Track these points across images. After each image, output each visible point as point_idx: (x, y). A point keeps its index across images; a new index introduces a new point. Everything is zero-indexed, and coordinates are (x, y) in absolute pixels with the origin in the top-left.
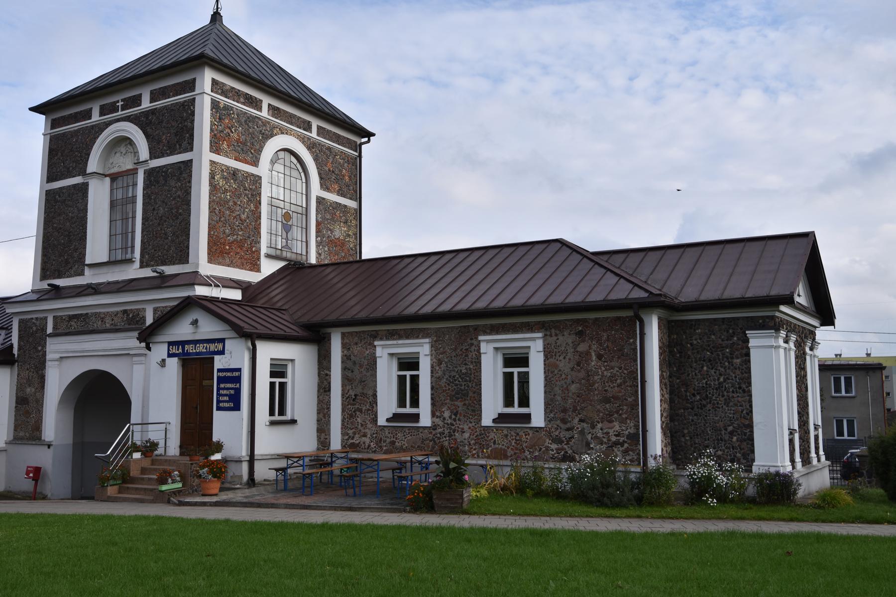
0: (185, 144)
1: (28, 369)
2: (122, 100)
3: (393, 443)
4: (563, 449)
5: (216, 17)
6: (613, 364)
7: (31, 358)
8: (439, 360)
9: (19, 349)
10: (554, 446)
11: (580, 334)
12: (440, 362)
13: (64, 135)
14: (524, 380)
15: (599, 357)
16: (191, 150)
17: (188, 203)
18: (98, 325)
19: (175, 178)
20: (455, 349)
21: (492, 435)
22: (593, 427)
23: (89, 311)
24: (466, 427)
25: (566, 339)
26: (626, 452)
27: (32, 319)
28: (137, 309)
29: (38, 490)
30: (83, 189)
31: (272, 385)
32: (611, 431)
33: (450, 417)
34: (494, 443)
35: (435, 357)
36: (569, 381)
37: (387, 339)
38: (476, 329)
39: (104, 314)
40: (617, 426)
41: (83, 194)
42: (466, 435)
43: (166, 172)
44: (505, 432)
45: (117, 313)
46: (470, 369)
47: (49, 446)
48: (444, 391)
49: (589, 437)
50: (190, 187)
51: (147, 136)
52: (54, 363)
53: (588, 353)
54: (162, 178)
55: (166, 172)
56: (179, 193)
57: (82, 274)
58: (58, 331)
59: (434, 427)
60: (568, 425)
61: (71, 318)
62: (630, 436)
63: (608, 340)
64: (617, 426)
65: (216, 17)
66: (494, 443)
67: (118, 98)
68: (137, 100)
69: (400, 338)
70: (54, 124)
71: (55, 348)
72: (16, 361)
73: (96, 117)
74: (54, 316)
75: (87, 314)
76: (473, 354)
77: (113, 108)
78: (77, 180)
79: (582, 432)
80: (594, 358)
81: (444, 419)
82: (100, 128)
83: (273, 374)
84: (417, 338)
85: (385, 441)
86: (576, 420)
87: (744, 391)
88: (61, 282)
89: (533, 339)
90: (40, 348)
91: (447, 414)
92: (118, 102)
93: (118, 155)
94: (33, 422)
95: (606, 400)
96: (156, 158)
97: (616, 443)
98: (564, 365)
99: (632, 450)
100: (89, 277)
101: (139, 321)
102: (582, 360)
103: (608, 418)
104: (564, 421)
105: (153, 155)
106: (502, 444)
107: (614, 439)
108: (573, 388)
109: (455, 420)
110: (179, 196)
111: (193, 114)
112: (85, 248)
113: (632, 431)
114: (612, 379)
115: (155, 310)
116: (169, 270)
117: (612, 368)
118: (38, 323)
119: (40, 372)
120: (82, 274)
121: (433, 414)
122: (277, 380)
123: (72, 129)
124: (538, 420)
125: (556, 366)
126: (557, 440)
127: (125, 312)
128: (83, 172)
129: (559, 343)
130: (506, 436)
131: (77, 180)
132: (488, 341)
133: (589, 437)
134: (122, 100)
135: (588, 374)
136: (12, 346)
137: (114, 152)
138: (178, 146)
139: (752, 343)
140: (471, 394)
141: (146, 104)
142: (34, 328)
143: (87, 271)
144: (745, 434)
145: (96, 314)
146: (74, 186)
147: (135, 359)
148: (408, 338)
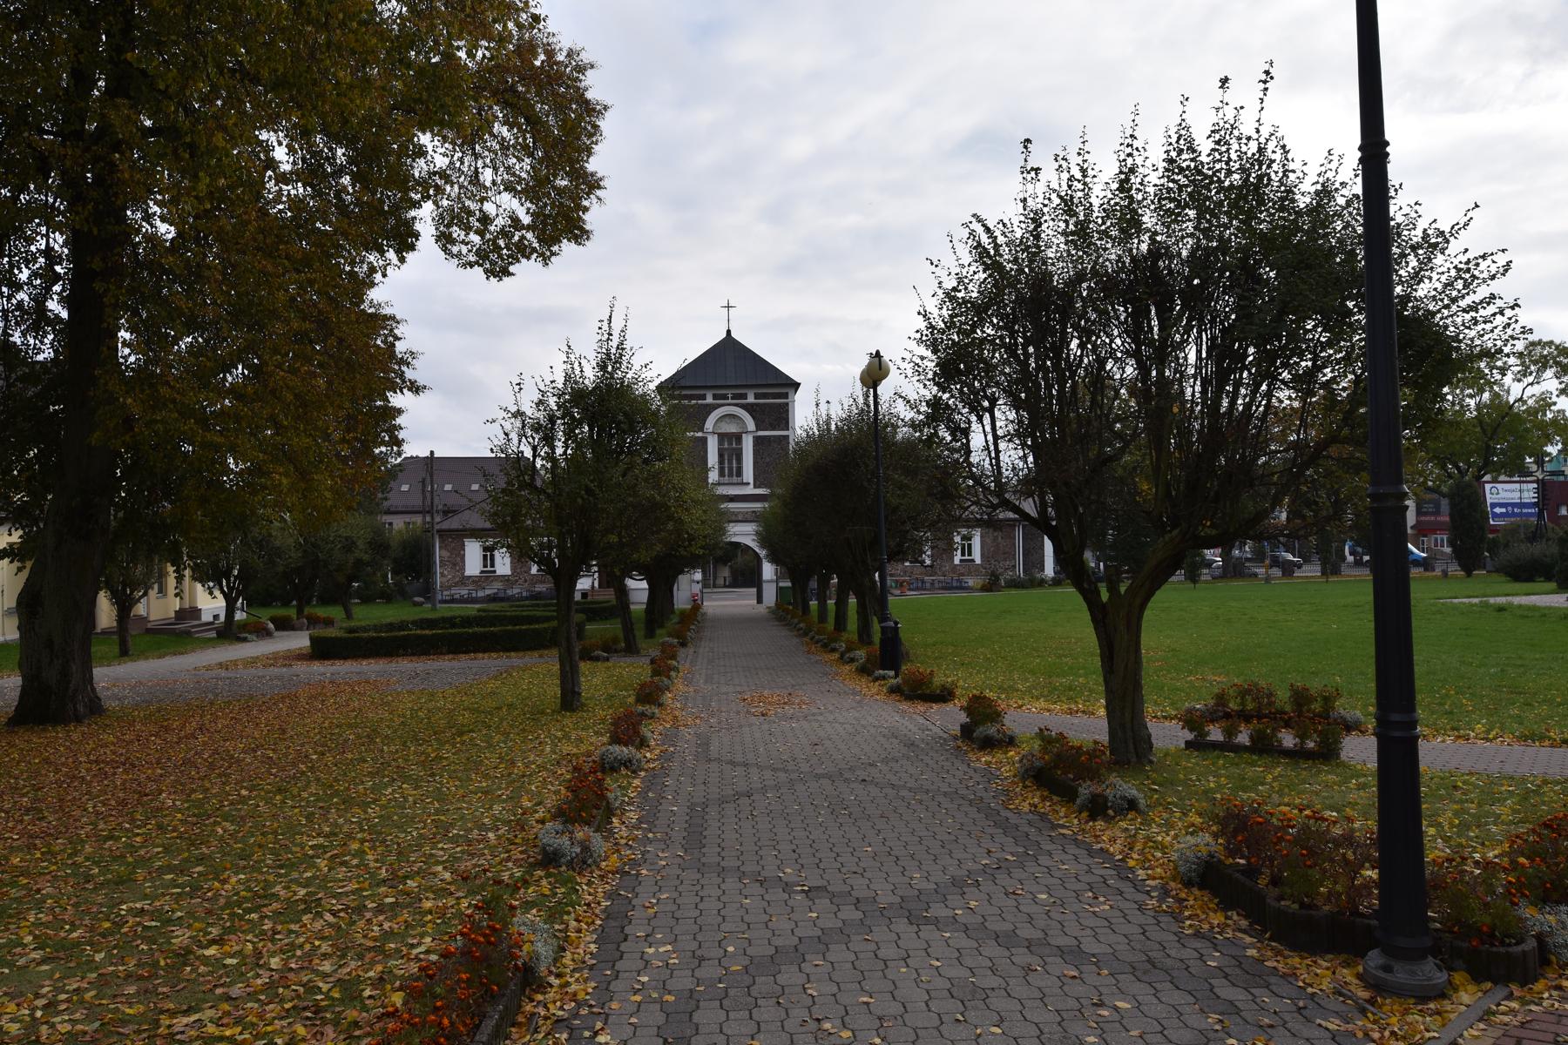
0: (782, 426)
5: (729, 332)
14: (970, 545)
18: (734, 518)
30: (704, 441)
51: (754, 418)
65: (729, 332)
67: (730, 393)
68: (744, 396)
77: (725, 397)
95: (1004, 553)
98: (988, 541)
102: (995, 539)
103: (1005, 560)
105: (758, 428)
111: (788, 411)
124: (978, 561)
128: (701, 429)
141: (751, 399)
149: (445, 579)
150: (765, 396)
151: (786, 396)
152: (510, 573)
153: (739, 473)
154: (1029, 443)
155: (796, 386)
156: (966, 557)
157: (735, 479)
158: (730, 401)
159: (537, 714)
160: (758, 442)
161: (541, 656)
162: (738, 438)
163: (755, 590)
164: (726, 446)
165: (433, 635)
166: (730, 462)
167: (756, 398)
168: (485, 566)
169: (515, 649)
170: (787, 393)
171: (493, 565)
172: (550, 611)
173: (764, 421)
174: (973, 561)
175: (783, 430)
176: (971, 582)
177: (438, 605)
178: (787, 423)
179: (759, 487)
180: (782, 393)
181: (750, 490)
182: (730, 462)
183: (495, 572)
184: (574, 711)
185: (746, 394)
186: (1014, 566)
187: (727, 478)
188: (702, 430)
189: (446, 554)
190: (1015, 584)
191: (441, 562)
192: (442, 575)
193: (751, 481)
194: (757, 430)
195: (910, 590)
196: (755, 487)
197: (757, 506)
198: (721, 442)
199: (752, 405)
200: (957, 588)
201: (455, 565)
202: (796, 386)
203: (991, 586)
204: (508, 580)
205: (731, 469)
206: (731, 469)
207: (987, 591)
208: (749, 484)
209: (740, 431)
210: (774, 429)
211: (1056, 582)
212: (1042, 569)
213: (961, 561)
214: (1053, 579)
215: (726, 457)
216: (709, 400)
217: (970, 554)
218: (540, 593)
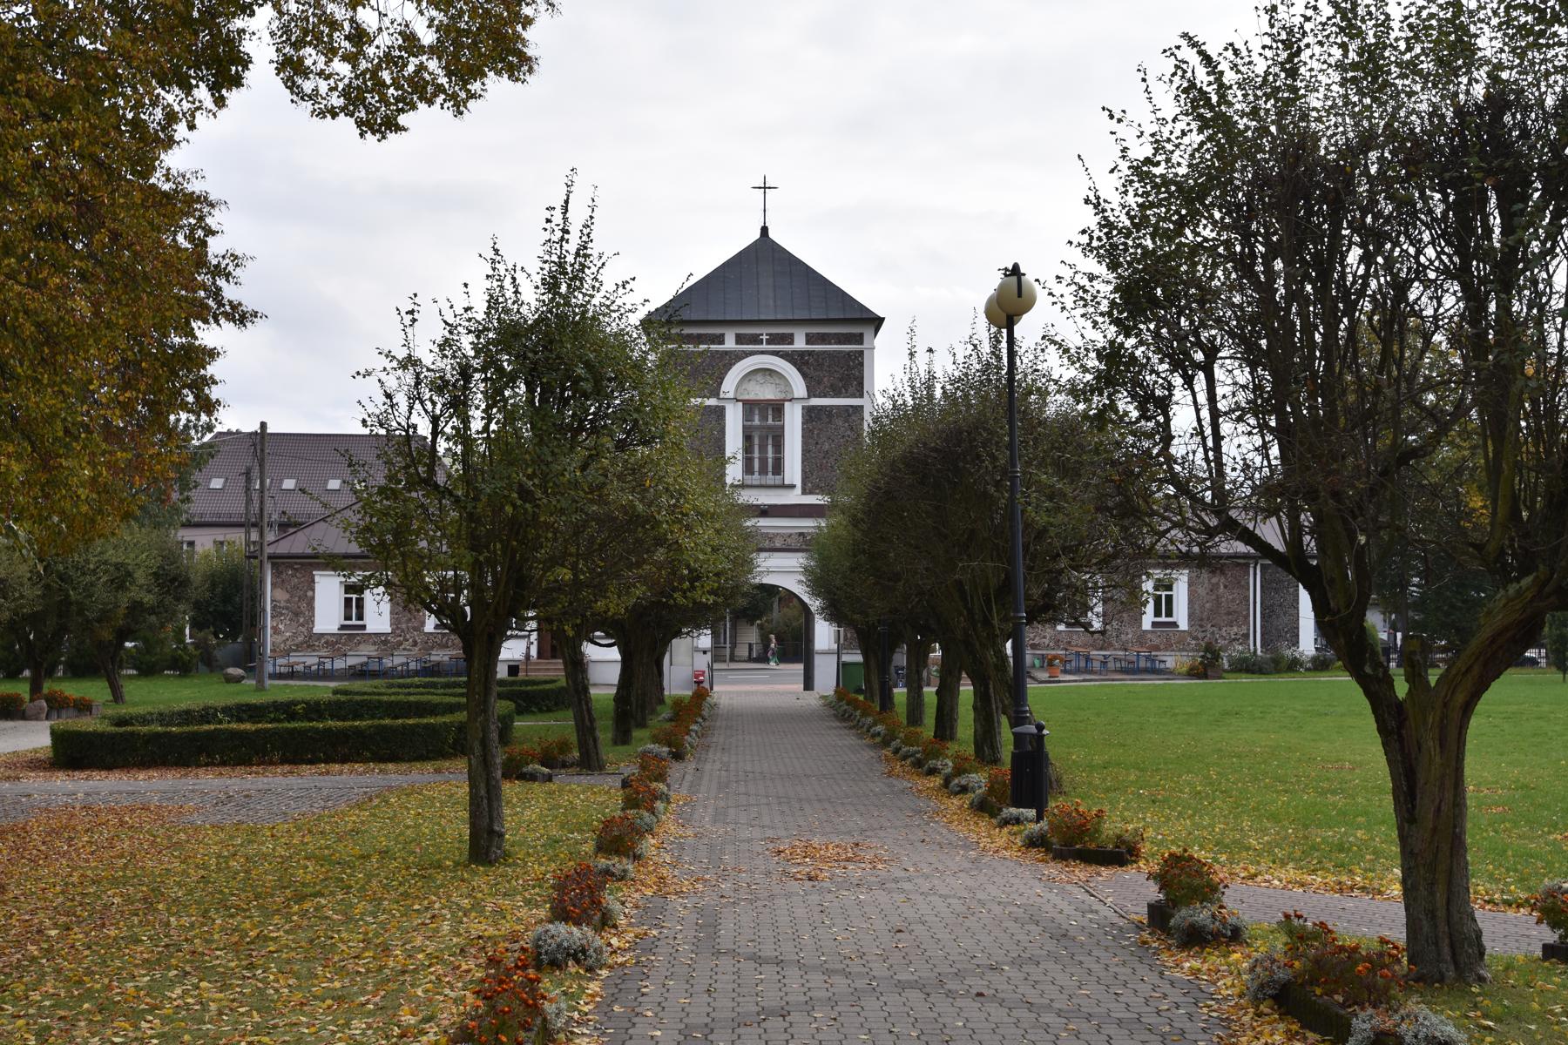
0: (851, 390)
5: (764, 230)
14: (1169, 599)
15: (1225, 587)
16: (862, 396)
18: (767, 544)
30: (719, 413)
40: (1235, 629)
45: (790, 535)
51: (804, 375)
53: (1218, 584)
55: (830, 412)
64: (1235, 629)
65: (764, 230)
67: (764, 332)
68: (789, 339)
73: (730, 344)
77: (756, 339)
78: (712, 402)
95: (1229, 613)
96: (815, 396)
98: (1202, 591)
102: (1213, 589)
104: (1201, 626)
106: (1156, 641)
108: (1208, 605)
111: (862, 364)
114: (1233, 600)
124: (1184, 625)
126: (1195, 638)
127: (801, 534)
131: (712, 402)
141: (800, 344)
149: (279, 639)
150: (823, 339)
151: (859, 339)
152: (389, 630)
153: (778, 468)
154: (1273, 423)
155: (877, 322)
156: (1163, 619)
157: (770, 479)
158: (764, 347)
159: (428, 869)
160: (811, 415)
161: (437, 771)
162: (777, 408)
163: (800, 667)
164: (757, 422)
165: (257, 731)
166: (763, 449)
167: (808, 342)
168: (348, 617)
169: (394, 758)
170: (861, 335)
171: (360, 617)
172: (454, 695)
174: (1174, 624)
175: (853, 396)
176: (1170, 661)
177: (268, 682)
178: (861, 384)
181: (795, 497)
182: (763, 449)
183: (364, 627)
184: (491, 863)
185: (792, 335)
186: (1246, 636)
187: (756, 476)
189: (282, 596)
190: (1247, 666)
191: (274, 608)
192: (275, 630)
193: (798, 482)
194: (809, 397)
195: (1065, 672)
196: (804, 492)
197: (807, 524)
198: (748, 415)
199: (802, 354)
200: (1146, 671)
201: (297, 614)
202: (877, 322)
203: (1206, 668)
204: (385, 642)
205: (763, 461)
206: (763, 461)
207: (1205, 676)
208: (793, 487)
209: (779, 396)
210: (837, 395)
211: (1320, 665)
212: (1295, 641)
213: (1154, 624)
214: (1314, 660)
215: (756, 441)
216: (730, 344)
217: (1169, 613)
218: (438, 664)
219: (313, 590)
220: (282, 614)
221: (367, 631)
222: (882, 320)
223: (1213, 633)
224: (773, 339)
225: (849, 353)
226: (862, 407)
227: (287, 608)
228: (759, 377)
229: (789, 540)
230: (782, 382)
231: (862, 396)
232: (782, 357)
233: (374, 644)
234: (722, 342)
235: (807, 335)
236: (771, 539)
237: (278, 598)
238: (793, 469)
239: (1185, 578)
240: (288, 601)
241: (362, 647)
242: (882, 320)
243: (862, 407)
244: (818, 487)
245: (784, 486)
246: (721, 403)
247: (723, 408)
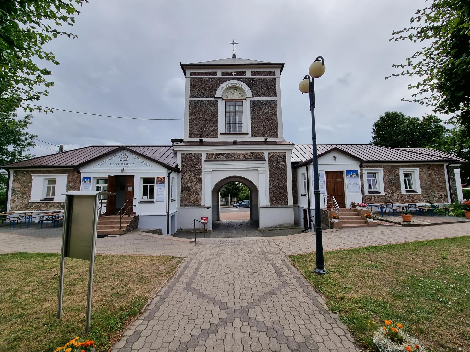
1: (189, 175)
2: (235, 72)
3: (371, 200)
4: (427, 200)
6: (438, 176)
7: (191, 170)
8: (385, 175)
9: (182, 166)
10: (424, 199)
11: (429, 168)
12: (386, 175)
13: (195, 80)
15: (435, 175)
16: (276, 96)
17: (276, 116)
19: (268, 106)
20: (390, 172)
21: (405, 197)
22: (435, 193)
23: (230, 152)
24: (396, 195)
25: (425, 170)
26: (444, 200)
27: (192, 153)
28: (259, 153)
29: (206, 228)
31: (405, 180)
32: (440, 195)
33: (391, 192)
34: (405, 199)
35: (384, 174)
36: (427, 181)
37: (366, 168)
38: (397, 166)
39: (239, 153)
40: (441, 193)
41: (215, 105)
42: (396, 197)
43: (263, 103)
44: (409, 195)
45: (247, 154)
46: (396, 178)
47: (208, 208)
48: (388, 184)
49: (434, 196)
50: (277, 110)
51: (251, 88)
52: (208, 173)
54: (260, 105)
55: (263, 103)
56: (271, 111)
57: (216, 136)
58: (209, 159)
59: (385, 195)
60: (428, 193)
61: (217, 154)
62: (445, 195)
63: (437, 170)
66: (405, 199)
67: (234, 71)
68: (244, 74)
69: (371, 167)
70: (192, 74)
71: (206, 167)
72: (180, 171)
73: (219, 76)
74: (206, 153)
75: (228, 153)
76: (397, 173)
77: (230, 74)
78: (212, 99)
79: (432, 195)
80: (433, 175)
81: (389, 192)
82: (221, 82)
83: (405, 177)
84: (377, 168)
85: (368, 200)
86: (430, 191)
87: (454, 184)
88: (204, 140)
89: (416, 169)
90: (197, 166)
91: (389, 191)
92: (233, 72)
93: (229, 93)
94: (194, 198)
95: (438, 186)
97: (441, 198)
98: (425, 177)
99: (446, 199)
100: (220, 138)
101: (260, 157)
102: (430, 175)
104: (427, 192)
105: (254, 95)
106: (408, 199)
107: (440, 196)
108: (428, 183)
109: (392, 193)
110: (271, 113)
112: (217, 126)
113: (445, 194)
114: (439, 180)
115: (269, 154)
116: (269, 139)
117: (439, 178)
118: (195, 156)
119: (198, 177)
120: (216, 136)
121: (385, 191)
122: (407, 178)
123: (205, 78)
124: (419, 192)
125: (422, 177)
126: (425, 197)
127: (252, 153)
129: (423, 170)
130: (409, 197)
131: (212, 99)
132: (402, 169)
133: (434, 196)
134: (235, 72)
135: (432, 179)
136: (177, 165)
137: (227, 91)
138: (268, 94)
139: (455, 172)
140: (397, 185)
141: (249, 75)
142: (193, 158)
143: (219, 136)
144: (456, 194)
145: (234, 153)
146: (208, 101)
147: (259, 172)
148: (374, 168)
150: (259, 73)
151: (274, 74)
153: (241, 128)
154: (467, 97)
160: (254, 104)
171: (53, 194)
173: (258, 91)
175: (272, 96)
179: (255, 137)
180: (272, 72)
181: (248, 138)
183: (52, 199)
188: (214, 97)
189: (17, 185)
191: (13, 191)
192: (13, 201)
193: (250, 132)
196: (252, 136)
199: (250, 80)
201: (23, 194)
208: (248, 134)
219: (31, 183)
220: (17, 194)
221: (54, 201)
222: (283, 65)
223: (432, 195)
224: (238, 74)
225: (269, 80)
226: (276, 101)
227: (19, 191)
228: (232, 90)
229: (246, 156)
230: (241, 93)
231: (276, 96)
232: (241, 81)
233: (58, 207)
234: (216, 75)
235: (252, 72)
236: (238, 156)
237: (16, 186)
238: (247, 128)
239: (418, 171)
240: (19, 188)
241: (52, 208)
242: (283, 65)
243: (276, 101)
244: (258, 134)
245: (243, 134)
246: (215, 99)
247: (217, 101)
